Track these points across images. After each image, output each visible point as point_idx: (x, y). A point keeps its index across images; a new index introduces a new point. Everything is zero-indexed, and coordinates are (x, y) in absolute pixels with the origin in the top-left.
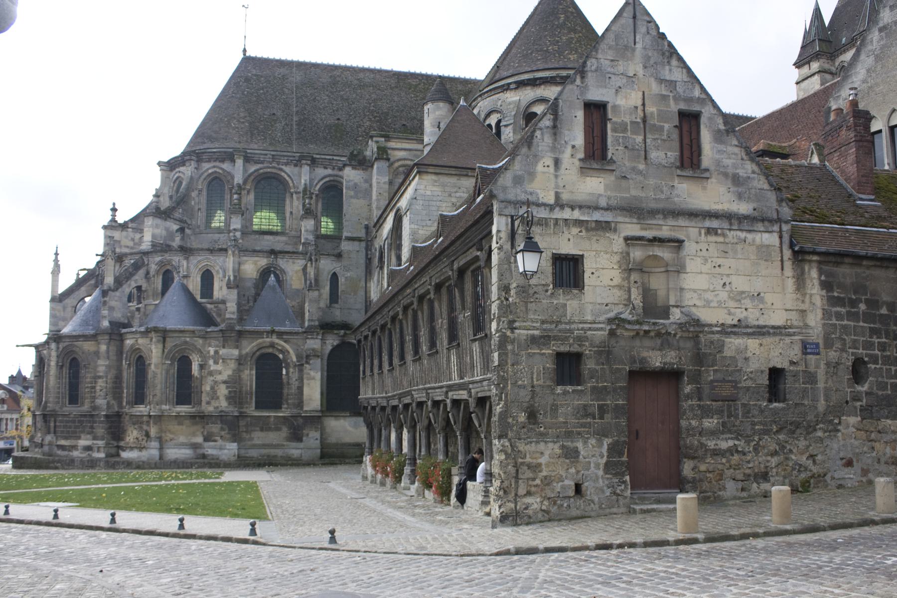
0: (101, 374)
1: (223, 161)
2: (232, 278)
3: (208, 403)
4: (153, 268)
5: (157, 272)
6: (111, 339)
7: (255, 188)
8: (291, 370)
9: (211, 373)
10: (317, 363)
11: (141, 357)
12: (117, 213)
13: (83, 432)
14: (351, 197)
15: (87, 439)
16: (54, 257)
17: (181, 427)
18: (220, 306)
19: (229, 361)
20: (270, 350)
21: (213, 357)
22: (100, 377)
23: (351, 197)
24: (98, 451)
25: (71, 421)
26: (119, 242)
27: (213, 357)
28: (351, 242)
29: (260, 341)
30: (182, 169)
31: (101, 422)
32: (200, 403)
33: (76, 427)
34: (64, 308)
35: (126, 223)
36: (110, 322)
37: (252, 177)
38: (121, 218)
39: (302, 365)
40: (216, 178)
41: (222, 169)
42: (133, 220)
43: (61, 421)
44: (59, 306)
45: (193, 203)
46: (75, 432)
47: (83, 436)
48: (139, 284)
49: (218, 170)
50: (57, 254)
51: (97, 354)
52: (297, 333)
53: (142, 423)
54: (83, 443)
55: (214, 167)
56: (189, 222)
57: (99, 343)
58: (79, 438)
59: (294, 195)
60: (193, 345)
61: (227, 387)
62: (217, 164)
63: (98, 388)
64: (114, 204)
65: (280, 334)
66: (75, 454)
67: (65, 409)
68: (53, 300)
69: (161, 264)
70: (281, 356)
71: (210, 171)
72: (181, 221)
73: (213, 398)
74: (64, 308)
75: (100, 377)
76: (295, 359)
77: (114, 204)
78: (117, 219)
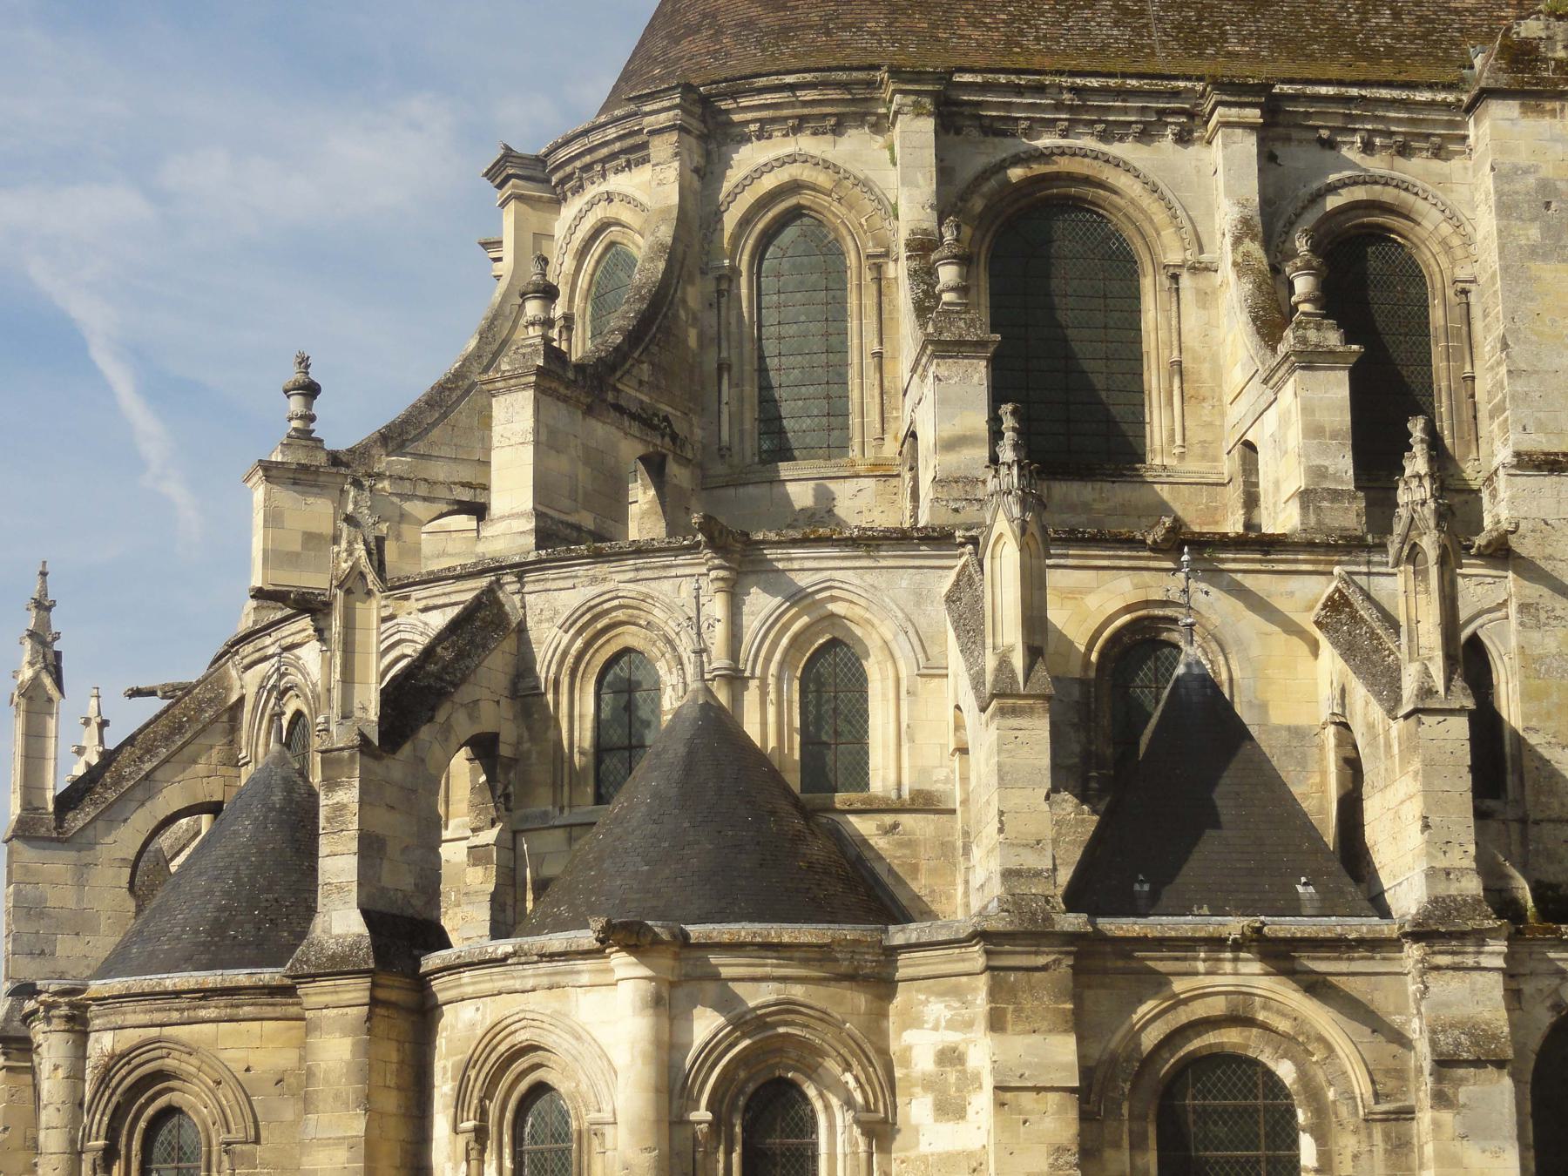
1: (838, 130)
2: (1018, 661)
4: (549, 640)
6: (374, 1002)
7: (994, 258)
8: (1347, 1144)
10: (1497, 1096)
11: (541, 1088)
12: (318, 406)
14: (1533, 252)
18: (906, 820)
19: (1027, 1099)
20: (1230, 1038)
21: (928, 1084)
23: (1533, 252)
27: (928, 1084)
28: (1549, 482)
30: (618, 182)
35: (361, 453)
36: (367, 914)
37: (978, 204)
38: (344, 424)
39: (1406, 1114)
40: (796, 213)
41: (827, 165)
42: (395, 437)
44: (55, 865)
45: (692, 341)
48: (486, 725)
50: (43, 606)
51: (298, 1086)
52: (1374, 945)
56: (680, 427)
57: (310, 1028)
59: (1186, 280)
60: (825, 1018)
62: (806, 143)
64: (304, 363)
65: (1280, 956)
68: (26, 831)
69: (594, 623)
70: (1286, 1071)
71: (769, 182)
72: (647, 421)
76: (1361, 1085)
77: (304, 363)
78: (318, 430)
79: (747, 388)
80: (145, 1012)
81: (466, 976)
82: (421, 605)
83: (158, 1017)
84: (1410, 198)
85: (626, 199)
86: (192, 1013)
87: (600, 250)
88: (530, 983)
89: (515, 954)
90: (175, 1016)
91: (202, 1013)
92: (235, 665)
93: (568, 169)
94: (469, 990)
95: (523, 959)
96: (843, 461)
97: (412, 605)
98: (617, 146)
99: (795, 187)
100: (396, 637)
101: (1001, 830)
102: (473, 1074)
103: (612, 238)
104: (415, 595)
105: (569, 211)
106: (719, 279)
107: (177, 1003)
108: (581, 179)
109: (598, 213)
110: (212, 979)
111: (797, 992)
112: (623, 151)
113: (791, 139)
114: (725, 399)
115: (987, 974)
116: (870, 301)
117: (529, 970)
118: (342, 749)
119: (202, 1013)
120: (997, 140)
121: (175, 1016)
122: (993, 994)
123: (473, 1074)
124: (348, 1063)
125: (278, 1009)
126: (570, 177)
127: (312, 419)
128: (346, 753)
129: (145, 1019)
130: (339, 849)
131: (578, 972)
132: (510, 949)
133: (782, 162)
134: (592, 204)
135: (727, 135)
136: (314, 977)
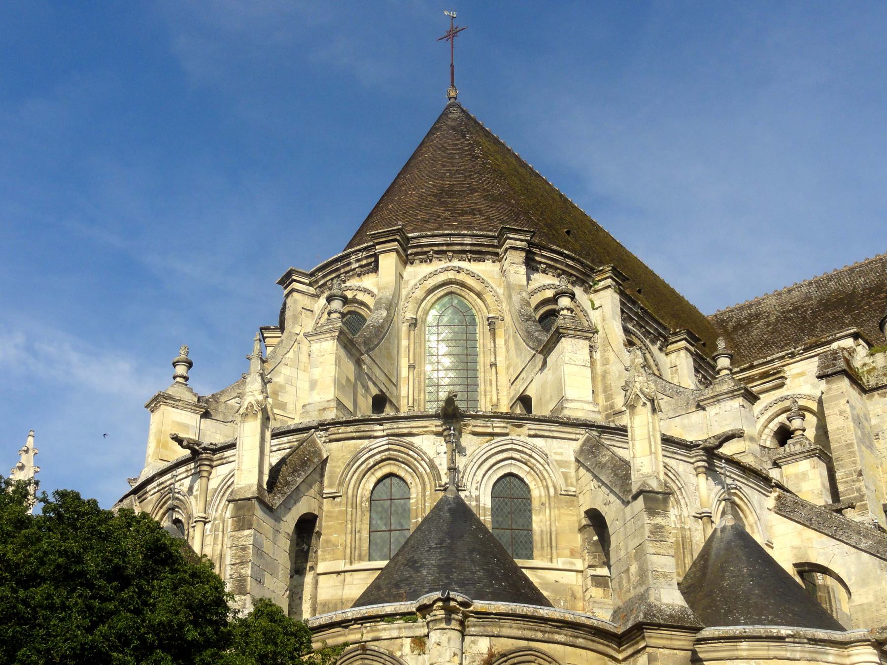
80: (519, 629)
81: (744, 645)
82: (532, 432)
86: (550, 636)
87: (443, 293)
88: (798, 655)
91: (557, 637)
93: (426, 249)
94: (744, 654)
95: (797, 640)
97: (525, 430)
98: (468, 248)
104: (528, 426)
107: (543, 627)
109: (451, 275)
112: (471, 252)
117: (799, 647)
118: (658, 493)
119: (557, 637)
121: (540, 635)
125: (595, 644)
128: (660, 496)
129: (519, 633)
130: (661, 551)
131: (828, 654)
132: (790, 632)
134: (446, 270)
136: (659, 626)
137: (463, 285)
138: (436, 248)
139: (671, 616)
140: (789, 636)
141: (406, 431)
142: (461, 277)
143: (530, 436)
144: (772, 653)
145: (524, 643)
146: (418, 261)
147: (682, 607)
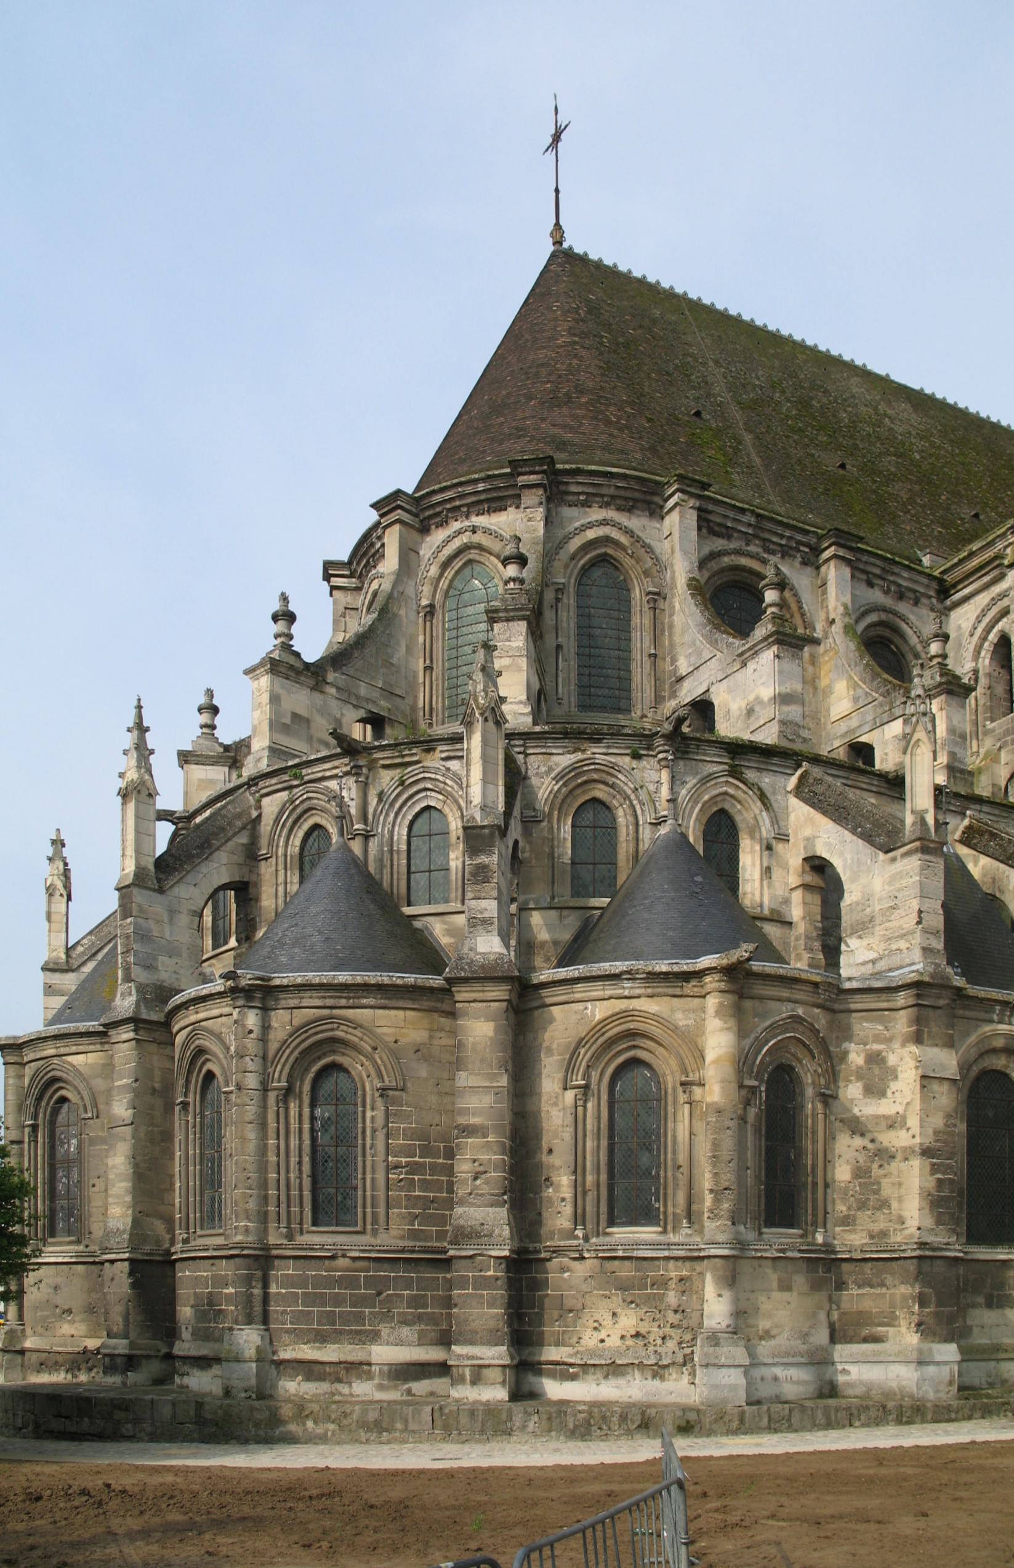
0: (475, 1120)
3: (847, 1221)
5: (560, 802)
9: (856, 1127)
12: (295, 629)
13: (387, 1317)
15: (400, 1343)
16: (129, 740)
17: (786, 1295)
22: (469, 1131)
24: (476, 1380)
25: (340, 1282)
26: (308, 721)
29: (987, 1028)
31: (483, 1283)
32: (822, 1219)
33: (357, 1301)
34: (172, 913)
43: (288, 1282)
46: (359, 1318)
47: (385, 1330)
49: (615, 534)
53: (664, 1283)
54: (383, 1353)
55: (604, 522)
58: (374, 1337)
61: (934, 1169)
63: (463, 1167)
66: (362, 1389)
67: (302, 1239)
71: (591, 534)
73: (862, 1205)
74: (172, 913)
75: (469, 1131)
77: (284, 598)
79: (572, 663)
80: (319, 998)
83: (329, 1002)
84: (898, 620)
85: (487, 531)
86: (356, 1001)
89: (628, 972)
90: (343, 1002)
91: (364, 1001)
92: (251, 794)
94: (578, 996)
96: (628, 717)
99: (607, 540)
100: (421, 776)
101: (919, 923)
102: (582, 1051)
103: (471, 556)
105: (439, 536)
106: (557, 590)
108: (447, 516)
110: (360, 977)
111: (800, 1011)
113: (604, 510)
114: (560, 667)
115: (915, 1009)
116: (647, 621)
120: (715, 538)
121: (343, 1002)
122: (918, 1021)
123: (582, 1051)
124: (491, 1039)
126: (438, 514)
127: (291, 637)
129: (318, 1002)
133: (604, 522)
134: (459, 533)
135: (563, 500)
137: (480, 547)
138: (448, 506)
139: (482, 966)
140: (622, 973)
141: (320, 775)
142: (478, 538)
143: (443, 759)
144: (608, 993)
145: (326, 1012)
146: (433, 527)
147: (500, 954)
